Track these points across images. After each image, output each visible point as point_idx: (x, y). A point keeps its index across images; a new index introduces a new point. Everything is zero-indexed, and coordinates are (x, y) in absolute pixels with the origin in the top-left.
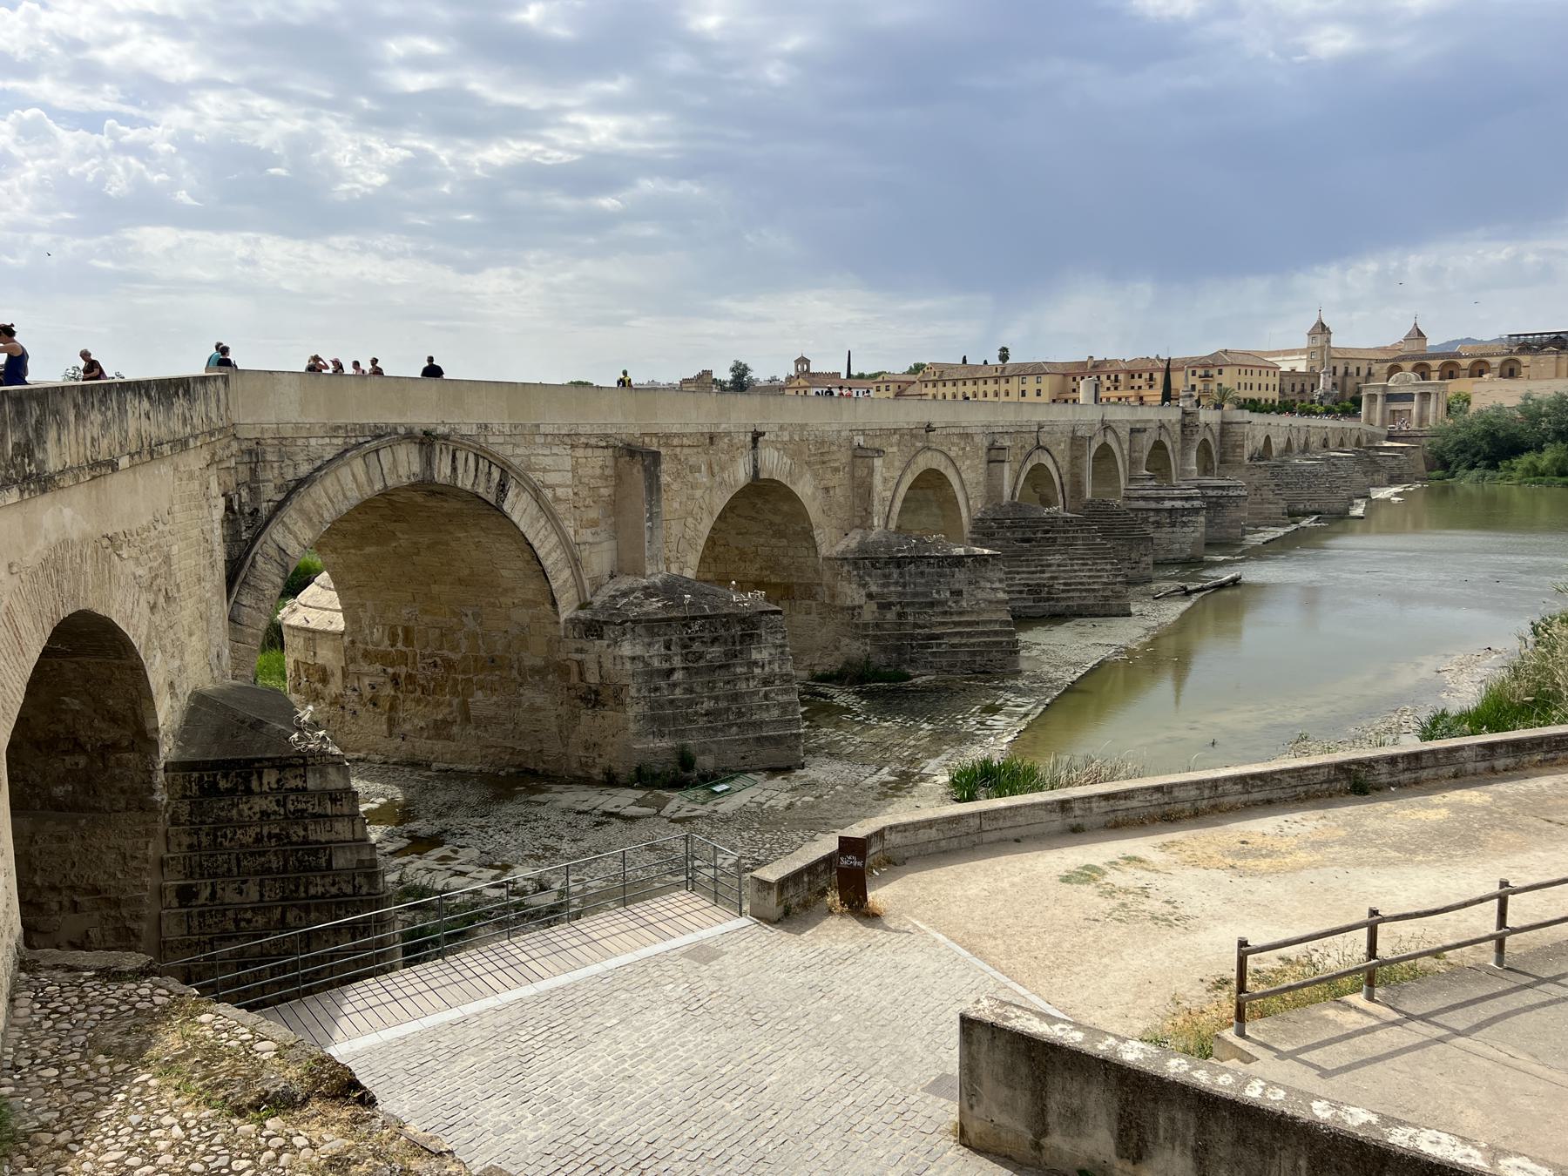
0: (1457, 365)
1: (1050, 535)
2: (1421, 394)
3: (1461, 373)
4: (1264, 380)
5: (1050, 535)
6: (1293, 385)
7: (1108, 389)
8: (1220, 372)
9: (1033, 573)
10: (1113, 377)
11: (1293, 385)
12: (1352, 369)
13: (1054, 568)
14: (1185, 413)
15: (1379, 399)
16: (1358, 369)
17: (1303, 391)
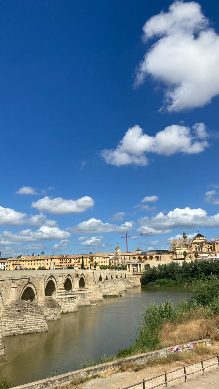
1: (26, 309)
2: (139, 264)
3: (148, 259)
5: (26, 309)
6: (113, 261)
8: (95, 258)
10: (70, 259)
11: (113, 261)
13: (27, 319)
14: (76, 271)
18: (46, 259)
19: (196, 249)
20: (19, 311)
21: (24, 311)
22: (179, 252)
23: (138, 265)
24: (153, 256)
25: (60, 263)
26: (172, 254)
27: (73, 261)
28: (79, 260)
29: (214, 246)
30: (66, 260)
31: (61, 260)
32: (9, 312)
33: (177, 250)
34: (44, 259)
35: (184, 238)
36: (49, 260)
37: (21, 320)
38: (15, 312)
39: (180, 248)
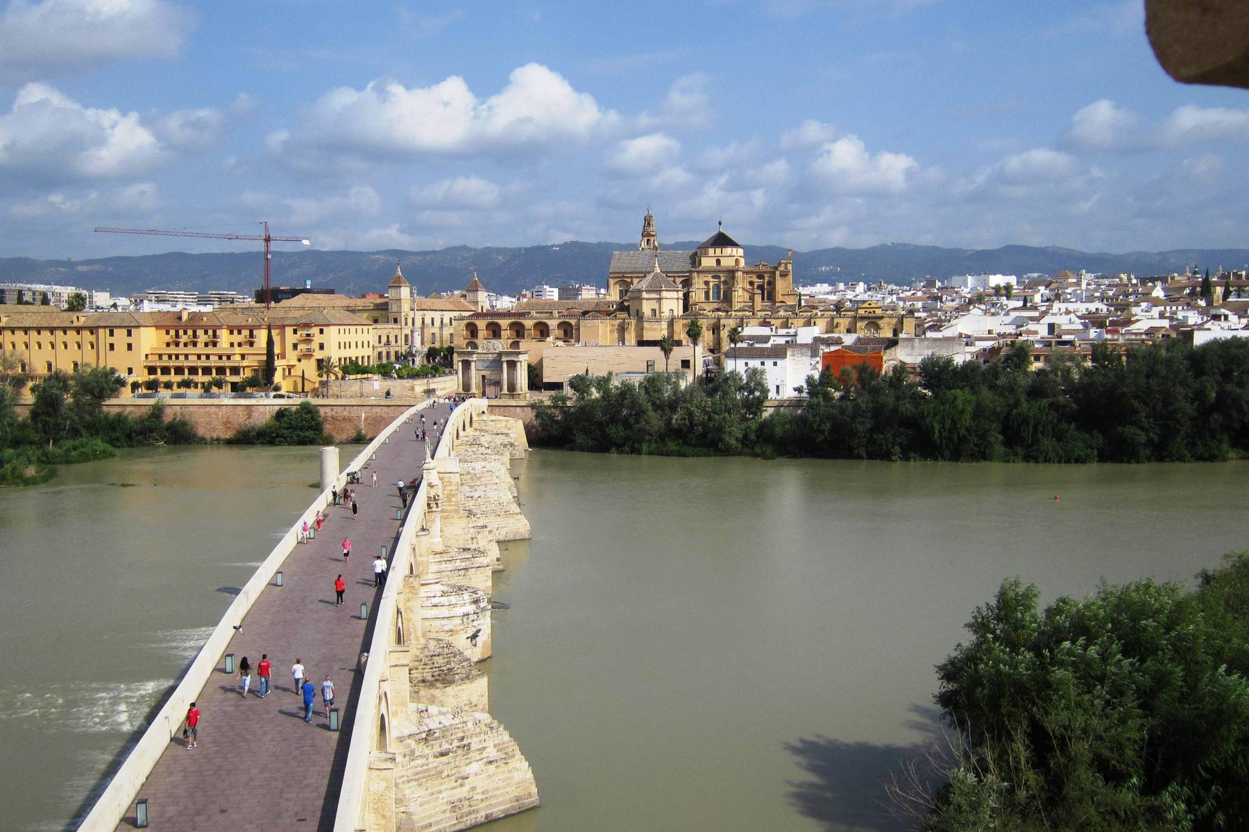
0: (522, 326)
1: (465, 742)
2: (508, 362)
3: (526, 333)
4: (360, 338)
5: (465, 742)
6: (380, 337)
7: (206, 345)
8: (321, 332)
9: (454, 788)
10: (210, 332)
11: (380, 337)
12: (428, 321)
15: (473, 365)
16: (433, 319)
17: (388, 343)
18: (105, 327)
19: (707, 293)
20: (442, 754)
21: (460, 752)
22: (654, 311)
23: (505, 365)
24: (549, 322)
25: (168, 345)
26: (625, 315)
27: (224, 335)
28: (251, 335)
29: (772, 283)
30: (195, 332)
31: (172, 332)
32: (413, 763)
33: (644, 301)
34: (98, 327)
35: (646, 239)
36: (120, 334)
37: (454, 784)
38: (431, 759)
39: (654, 296)
